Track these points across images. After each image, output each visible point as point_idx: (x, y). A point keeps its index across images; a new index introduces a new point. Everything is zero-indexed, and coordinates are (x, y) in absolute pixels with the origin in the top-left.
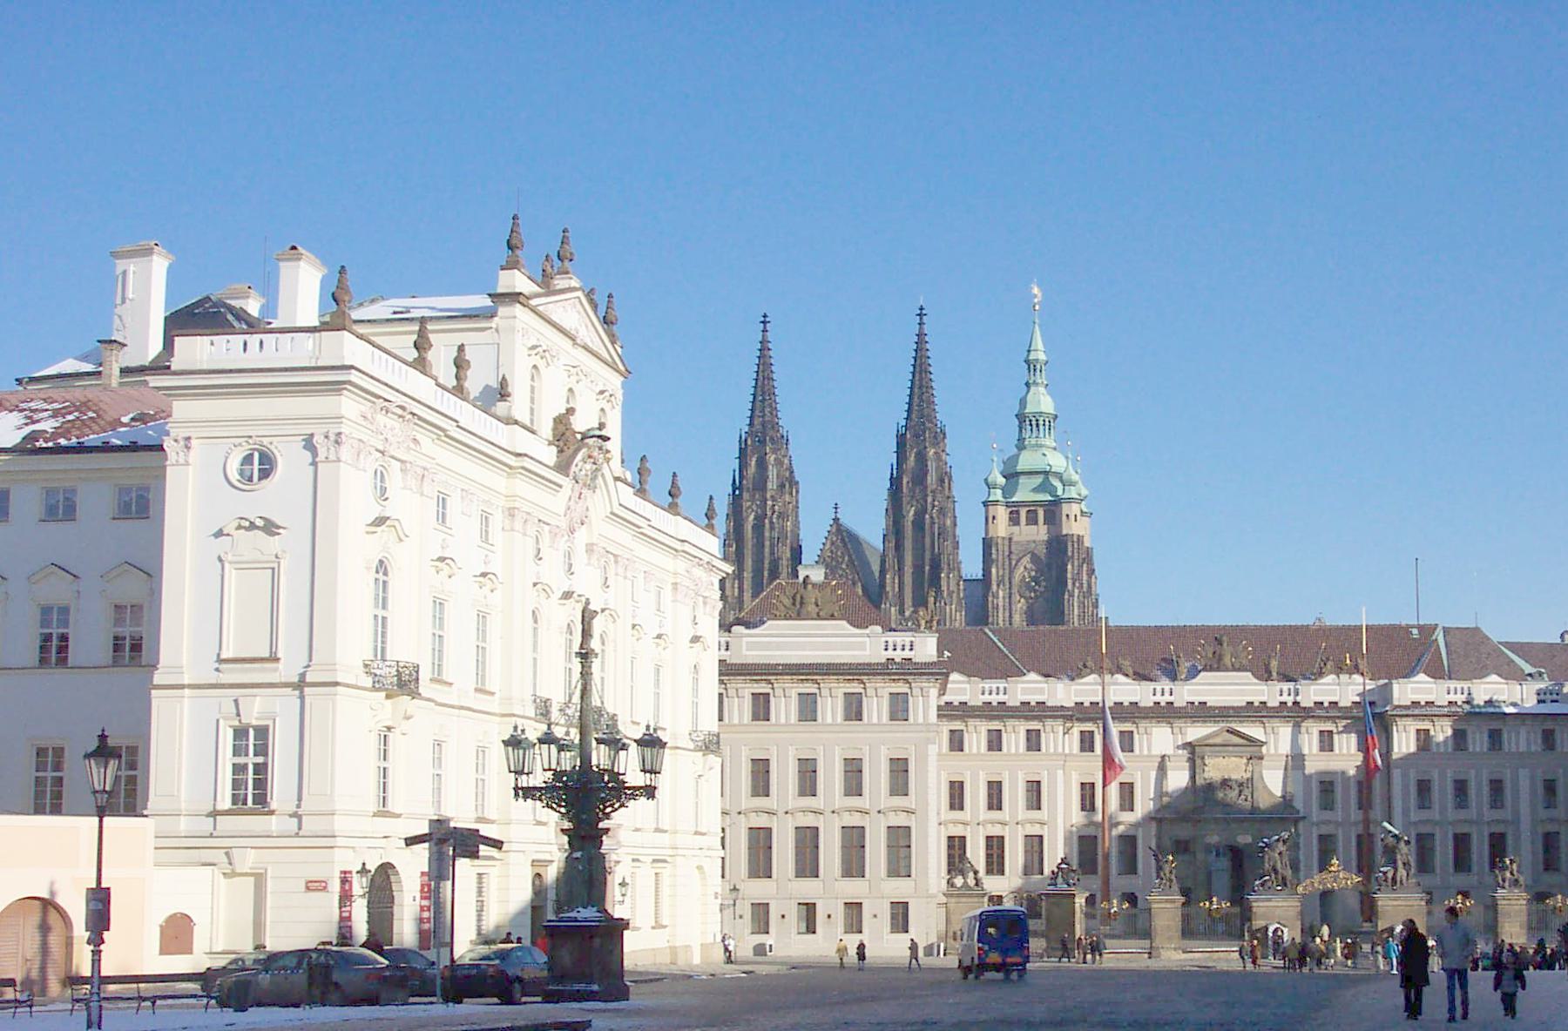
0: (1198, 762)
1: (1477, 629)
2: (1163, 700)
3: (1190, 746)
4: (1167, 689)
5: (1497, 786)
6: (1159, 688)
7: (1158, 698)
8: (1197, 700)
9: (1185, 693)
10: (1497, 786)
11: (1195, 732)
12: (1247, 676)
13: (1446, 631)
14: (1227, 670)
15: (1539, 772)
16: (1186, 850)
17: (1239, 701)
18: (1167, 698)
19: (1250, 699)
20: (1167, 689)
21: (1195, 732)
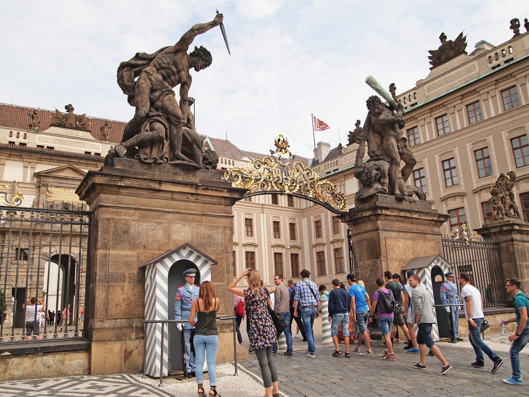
0: (43, 189)
1: (227, 142)
2: (17, 141)
3: (38, 175)
4: (22, 133)
5: (249, 222)
6: (15, 132)
7: (14, 139)
8: (46, 144)
9: (34, 140)
10: (249, 222)
11: (41, 168)
12: (88, 135)
13: (212, 140)
14: (72, 128)
15: (271, 216)
16: (26, 258)
17: (79, 149)
18: (21, 140)
19: (88, 150)
20: (22, 133)
21: (41, 168)
